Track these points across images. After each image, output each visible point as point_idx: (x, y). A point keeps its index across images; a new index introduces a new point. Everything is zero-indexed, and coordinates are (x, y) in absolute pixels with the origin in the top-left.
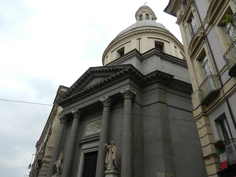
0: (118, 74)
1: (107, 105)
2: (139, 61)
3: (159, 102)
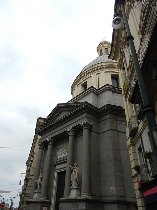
1: (72, 134)
2: (95, 96)
3: (111, 130)
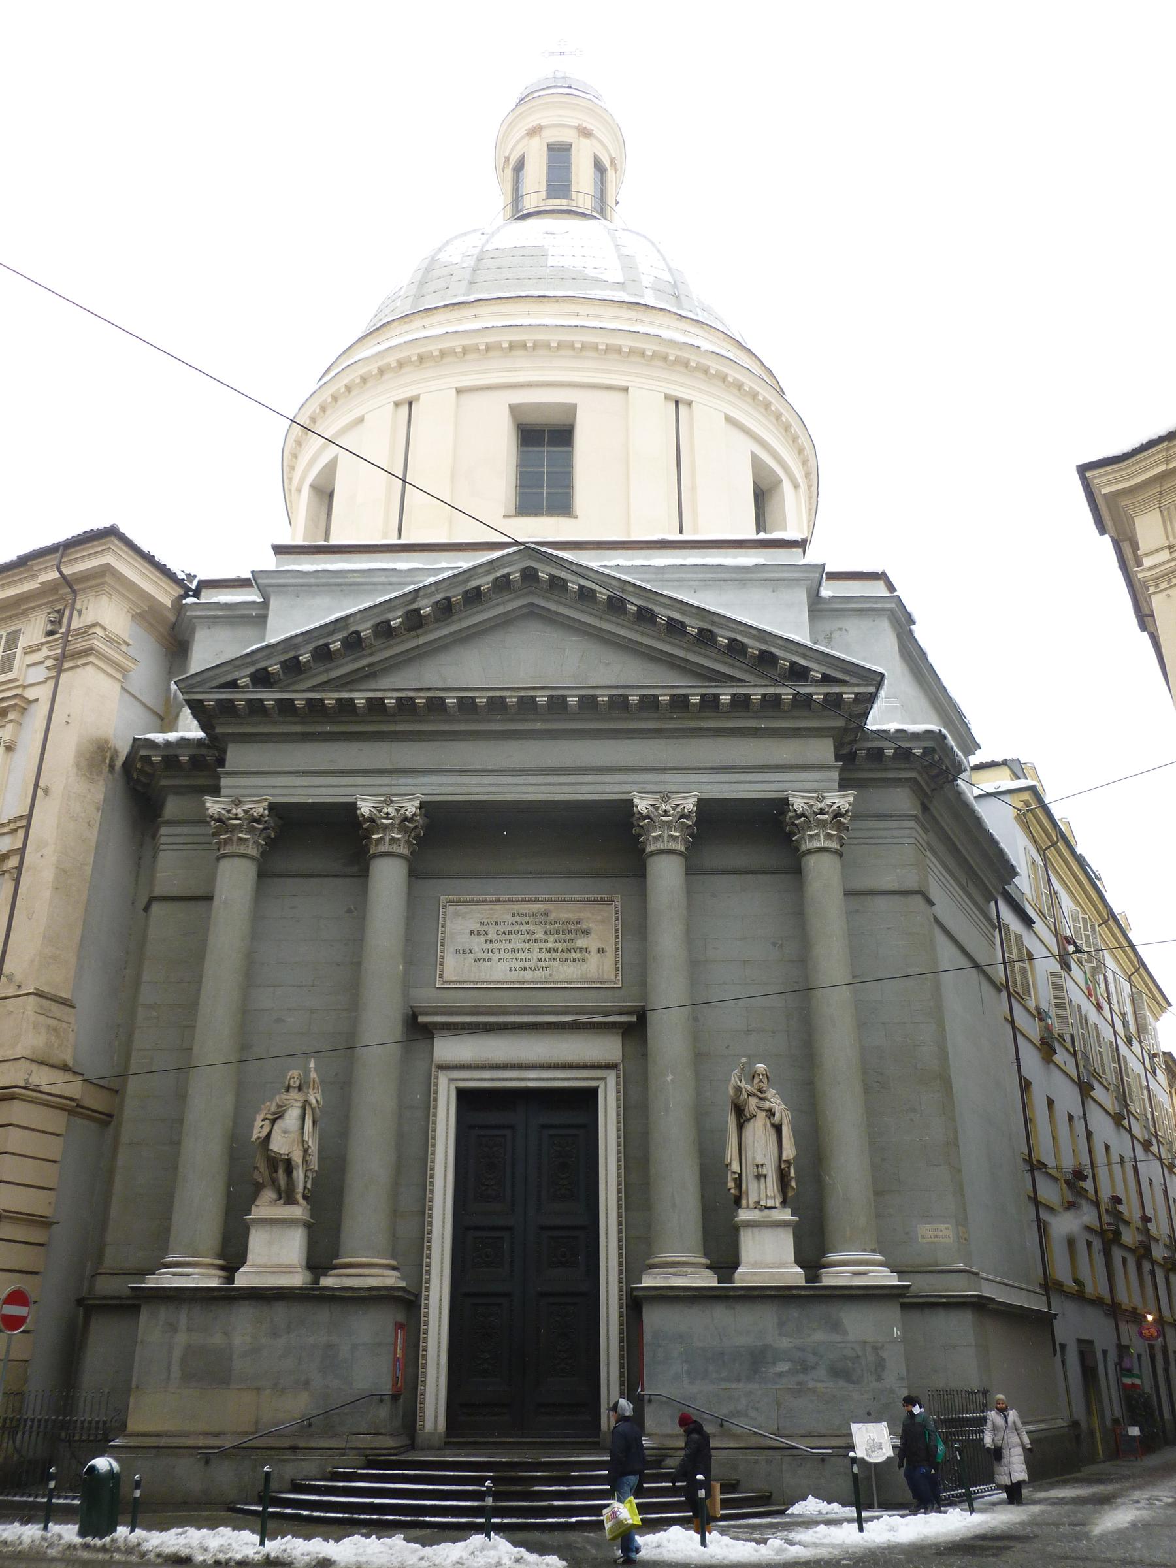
0: (786, 693)
1: (681, 847)
